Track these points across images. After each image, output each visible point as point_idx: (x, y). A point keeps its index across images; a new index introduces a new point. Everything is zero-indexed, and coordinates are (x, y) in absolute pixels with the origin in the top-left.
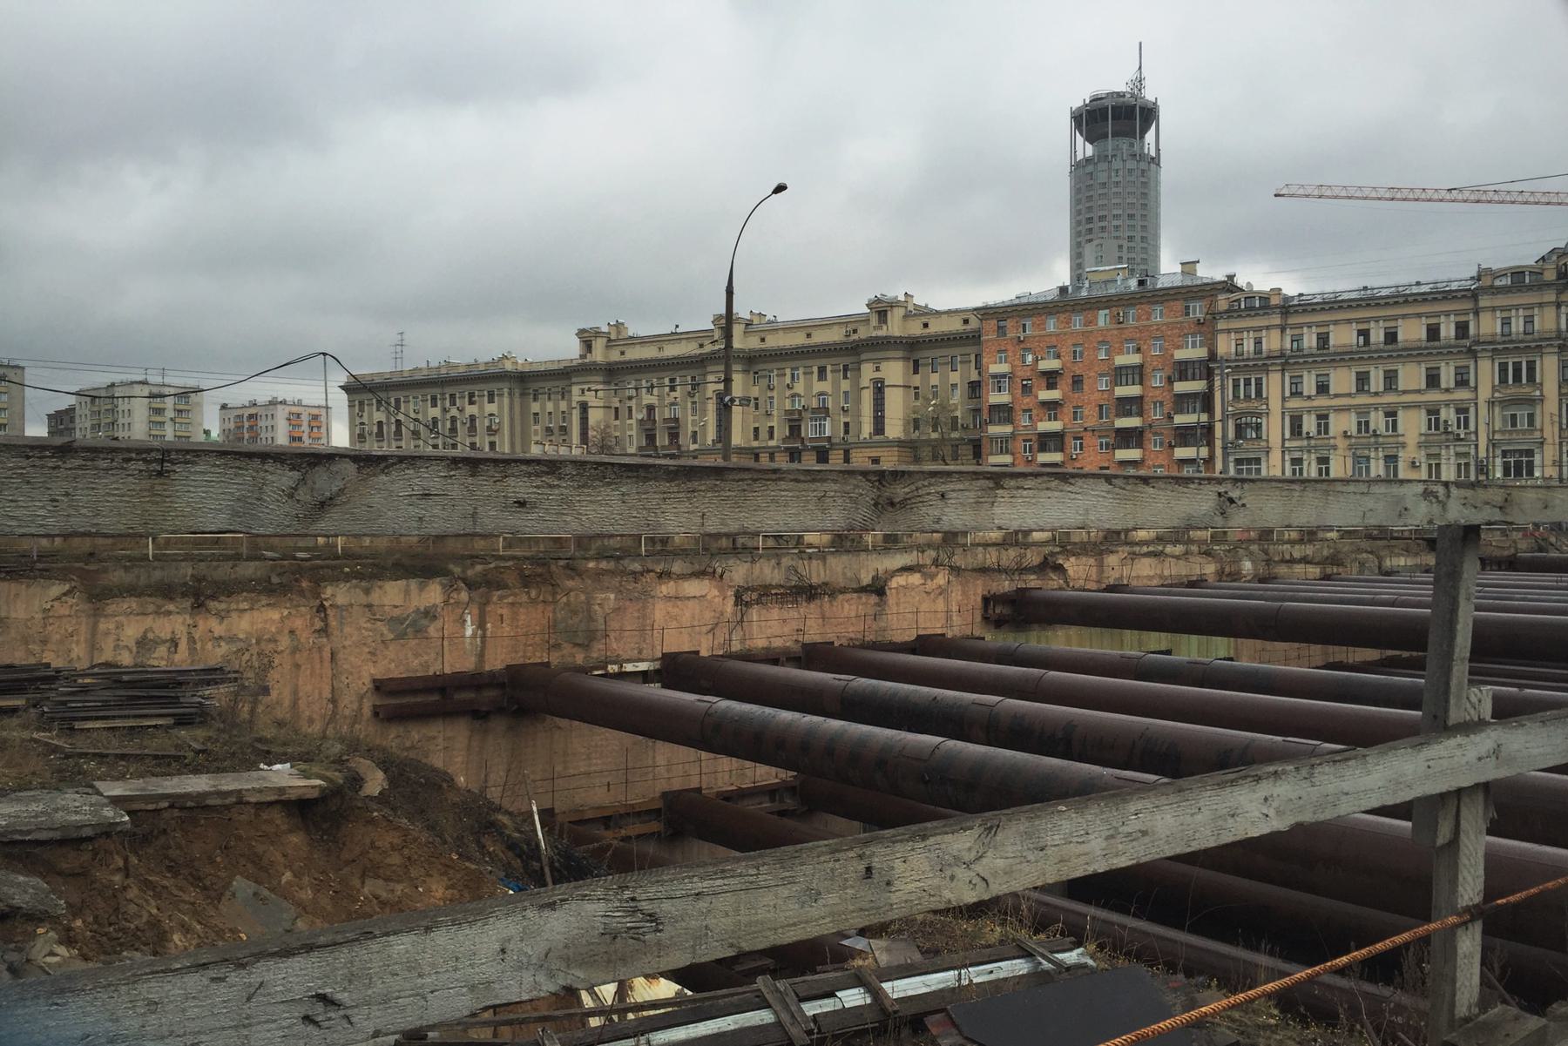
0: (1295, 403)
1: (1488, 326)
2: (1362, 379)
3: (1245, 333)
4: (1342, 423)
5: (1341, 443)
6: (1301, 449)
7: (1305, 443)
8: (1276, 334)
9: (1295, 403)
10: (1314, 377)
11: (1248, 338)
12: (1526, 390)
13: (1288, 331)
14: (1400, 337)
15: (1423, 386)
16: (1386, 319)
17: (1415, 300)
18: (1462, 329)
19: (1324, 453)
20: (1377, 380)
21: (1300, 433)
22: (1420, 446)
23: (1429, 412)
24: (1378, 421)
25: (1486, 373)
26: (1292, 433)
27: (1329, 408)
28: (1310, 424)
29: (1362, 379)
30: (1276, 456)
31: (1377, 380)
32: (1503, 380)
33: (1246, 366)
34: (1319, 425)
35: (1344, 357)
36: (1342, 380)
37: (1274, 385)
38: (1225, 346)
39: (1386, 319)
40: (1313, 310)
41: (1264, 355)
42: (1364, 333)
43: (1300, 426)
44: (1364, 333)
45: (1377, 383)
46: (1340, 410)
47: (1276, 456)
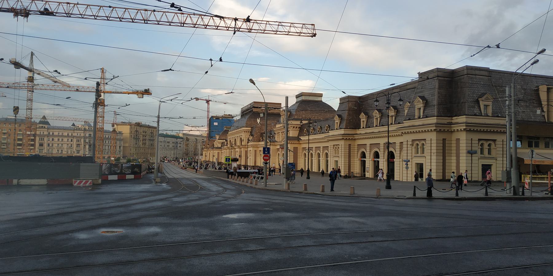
1: (75, 134)
2: (59, 139)
8: (46, 132)
18: (72, 134)
23: (67, 145)
24: (60, 145)
25: (75, 140)
28: (51, 145)
29: (59, 139)
30: (45, 149)
32: (77, 141)
35: (56, 136)
36: (56, 139)
37: (46, 139)
38: (38, 133)
47: (45, 149)
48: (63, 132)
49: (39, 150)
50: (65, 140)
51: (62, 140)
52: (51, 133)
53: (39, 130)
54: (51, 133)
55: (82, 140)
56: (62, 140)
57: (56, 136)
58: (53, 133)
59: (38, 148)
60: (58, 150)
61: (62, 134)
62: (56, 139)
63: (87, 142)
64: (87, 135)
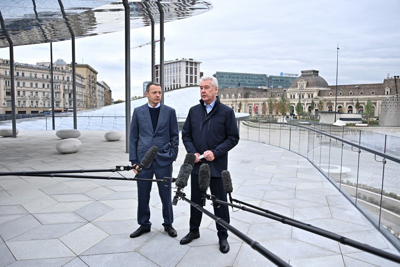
0: (19, 88)
2: (31, 84)
3: (7, 70)
4: (28, 94)
5: (28, 98)
6: (20, 99)
7: (21, 98)
9: (19, 88)
10: (22, 82)
11: (8, 71)
12: (58, 90)
13: (16, 71)
14: (25, 75)
15: (42, 87)
16: (35, 72)
17: (24, 67)
19: (25, 100)
20: (34, 86)
21: (20, 95)
22: (42, 100)
24: (34, 94)
26: (18, 95)
27: (26, 90)
28: (21, 93)
29: (31, 84)
31: (34, 86)
33: (7, 78)
34: (23, 93)
39: (35, 72)
40: (44, 70)
41: (59, 80)
42: (43, 75)
43: (20, 94)
44: (43, 75)
45: (46, 87)
46: (27, 91)
48: (37, 72)
49: (7, 101)
50: (28, 84)
51: (37, 84)
52: (20, 74)
53: (4, 68)
54: (20, 74)
55: (62, 86)
56: (37, 84)
57: (27, 79)
58: (23, 74)
59: (5, 99)
60: (32, 102)
61: (36, 75)
62: (28, 84)
63: (67, 90)
64: (66, 79)
